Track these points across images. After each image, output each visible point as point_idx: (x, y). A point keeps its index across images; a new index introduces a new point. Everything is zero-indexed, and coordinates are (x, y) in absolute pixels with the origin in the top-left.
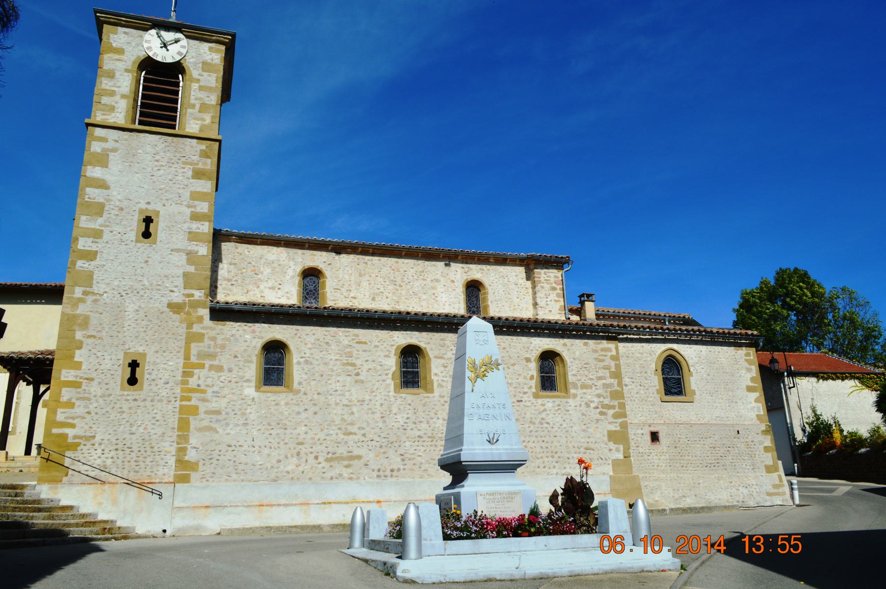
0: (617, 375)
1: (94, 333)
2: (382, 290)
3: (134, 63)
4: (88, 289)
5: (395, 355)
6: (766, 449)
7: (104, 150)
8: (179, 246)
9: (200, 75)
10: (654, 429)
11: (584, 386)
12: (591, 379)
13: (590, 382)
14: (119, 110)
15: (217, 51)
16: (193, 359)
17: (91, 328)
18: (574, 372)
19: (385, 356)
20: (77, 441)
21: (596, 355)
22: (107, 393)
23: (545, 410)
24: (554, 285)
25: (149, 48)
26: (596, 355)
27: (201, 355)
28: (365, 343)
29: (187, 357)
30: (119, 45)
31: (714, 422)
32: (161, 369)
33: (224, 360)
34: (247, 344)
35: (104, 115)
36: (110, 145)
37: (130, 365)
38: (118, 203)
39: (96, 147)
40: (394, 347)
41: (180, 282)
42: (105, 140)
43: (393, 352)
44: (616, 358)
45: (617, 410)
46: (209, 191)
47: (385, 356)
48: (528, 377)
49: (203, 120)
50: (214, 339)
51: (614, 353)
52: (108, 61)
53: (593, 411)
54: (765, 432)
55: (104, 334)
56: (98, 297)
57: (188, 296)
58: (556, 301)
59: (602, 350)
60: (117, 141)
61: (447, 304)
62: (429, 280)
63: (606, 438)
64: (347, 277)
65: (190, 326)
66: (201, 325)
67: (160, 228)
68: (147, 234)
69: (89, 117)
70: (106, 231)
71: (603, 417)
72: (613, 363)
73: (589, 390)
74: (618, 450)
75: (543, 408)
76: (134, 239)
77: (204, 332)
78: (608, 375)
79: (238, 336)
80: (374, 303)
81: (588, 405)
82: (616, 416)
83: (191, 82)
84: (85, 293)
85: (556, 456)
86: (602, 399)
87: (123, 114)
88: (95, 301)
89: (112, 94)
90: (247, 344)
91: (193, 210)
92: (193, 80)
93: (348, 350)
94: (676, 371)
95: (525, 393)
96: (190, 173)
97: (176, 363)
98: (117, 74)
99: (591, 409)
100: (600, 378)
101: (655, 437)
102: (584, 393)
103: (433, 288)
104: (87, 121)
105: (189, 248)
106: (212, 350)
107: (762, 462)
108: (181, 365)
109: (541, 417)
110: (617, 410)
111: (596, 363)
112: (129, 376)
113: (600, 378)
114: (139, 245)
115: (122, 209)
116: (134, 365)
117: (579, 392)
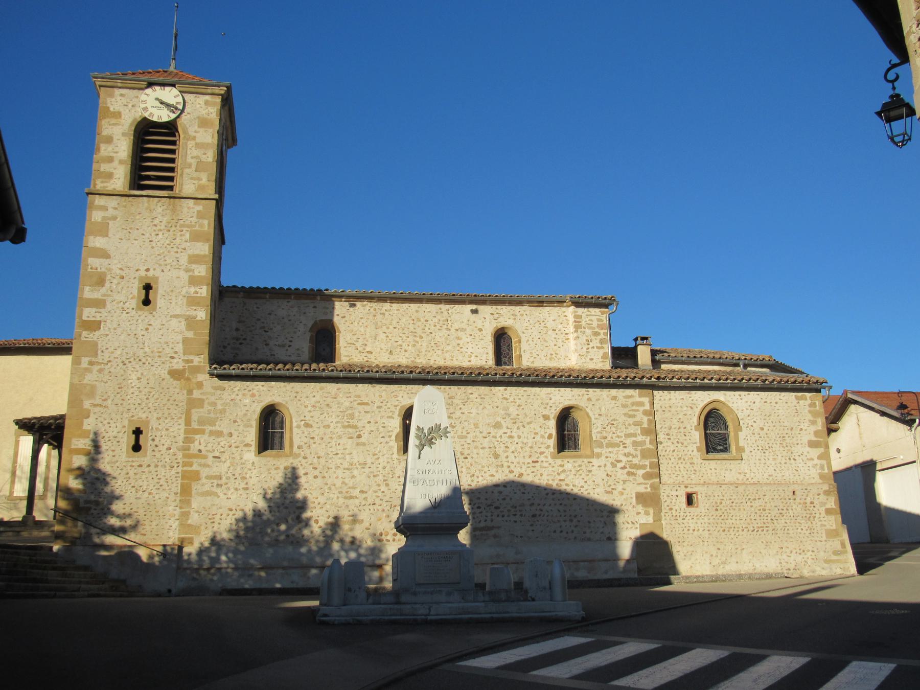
0: (652, 431)
1: (100, 402)
2: (400, 343)
3: (131, 124)
4: (93, 359)
5: (399, 415)
6: (829, 512)
7: (104, 218)
8: (178, 311)
9: (196, 132)
10: (689, 490)
11: (611, 445)
12: (618, 437)
13: (617, 440)
14: (117, 176)
15: (214, 104)
16: (195, 425)
17: (98, 397)
18: (599, 430)
19: (389, 417)
20: (88, 505)
21: (626, 410)
22: (114, 459)
23: (564, 471)
24: (597, 330)
25: (145, 109)
26: (626, 410)
27: (201, 422)
28: (367, 404)
29: (188, 422)
30: (117, 109)
31: (765, 481)
32: (165, 435)
33: (223, 426)
34: (246, 408)
35: (102, 182)
36: (111, 212)
37: (134, 432)
38: (118, 272)
39: (96, 216)
40: (398, 408)
41: (180, 348)
42: (105, 208)
43: (397, 413)
44: (652, 413)
45: (648, 469)
46: (207, 253)
47: (389, 417)
48: (546, 435)
49: (199, 179)
50: (214, 404)
51: (647, 407)
52: (107, 128)
53: (621, 471)
54: (827, 493)
55: (109, 402)
56: (102, 366)
57: (188, 361)
58: (597, 347)
59: (633, 404)
60: (116, 209)
61: (473, 355)
62: (453, 330)
63: (634, 500)
64: (362, 330)
65: (190, 392)
66: (200, 391)
67: (159, 296)
68: (147, 302)
69: (89, 186)
70: (109, 299)
71: (631, 478)
72: (645, 419)
73: (616, 449)
74: (647, 513)
75: (561, 469)
76: (135, 306)
77: (204, 397)
78: (639, 432)
79: (237, 401)
80: (392, 357)
81: (614, 465)
82: (647, 476)
83: (188, 140)
84: (91, 363)
85: (575, 520)
86: (630, 458)
87: (122, 180)
88: (100, 371)
89: (110, 160)
90: (246, 408)
91: (191, 274)
92: (189, 138)
93: (350, 412)
94: (723, 426)
95: (542, 453)
96: (188, 236)
97: (178, 429)
98: (115, 138)
99: (618, 469)
100: (628, 436)
101: (690, 500)
102: (610, 452)
103: (458, 338)
104: (86, 190)
105: (188, 313)
106: (212, 415)
107: (822, 525)
108: (182, 431)
109: (559, 478)
110: (648, 469)
111: (625, 418)
112: (133, 443)
113: (628, 436)
114: (140, 313)
115: (122, 278)
116: (138, 432)
117: (605, 451)
